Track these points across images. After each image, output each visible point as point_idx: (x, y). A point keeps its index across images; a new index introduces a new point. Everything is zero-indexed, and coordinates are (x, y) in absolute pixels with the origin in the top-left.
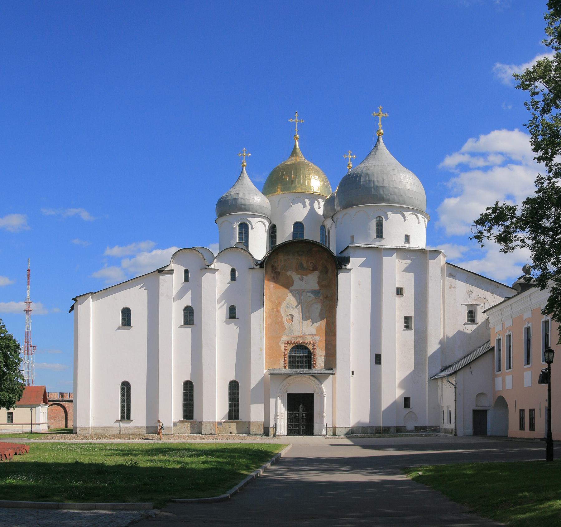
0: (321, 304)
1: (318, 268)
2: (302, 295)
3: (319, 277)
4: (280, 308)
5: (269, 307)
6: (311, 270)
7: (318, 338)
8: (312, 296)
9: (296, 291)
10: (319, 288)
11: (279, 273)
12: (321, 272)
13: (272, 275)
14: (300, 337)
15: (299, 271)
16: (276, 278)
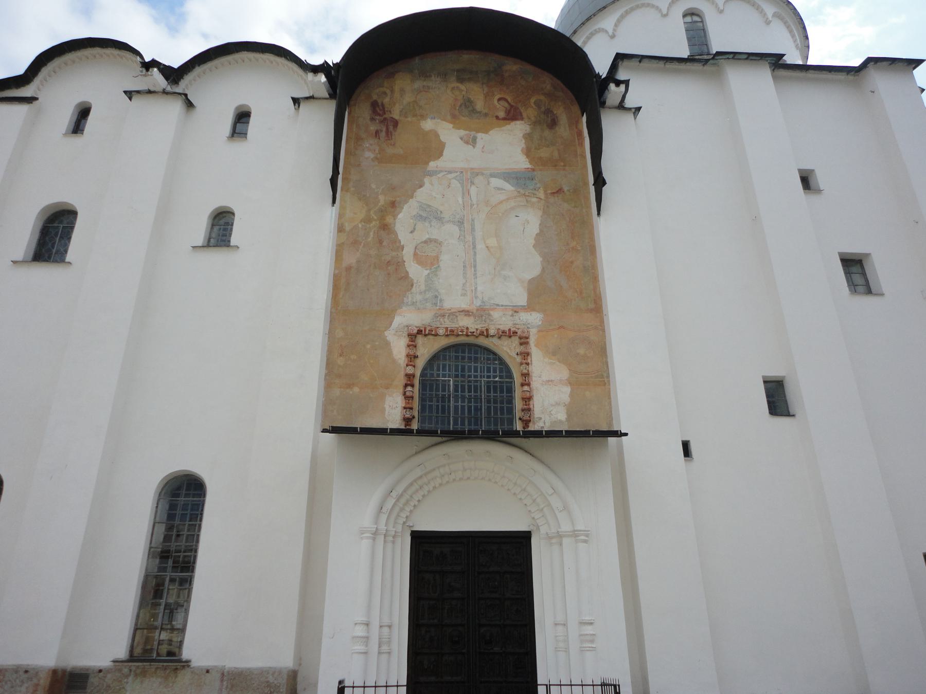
0: (540, 213)
1: (524, 115)
2: (472, 183)
3: (528, 137)
4: (395, 219)
5: (355, 214)
6: (500, 117)
7: (533, 319)
8: (508, 187)
9: (450, 172)
10: (530, 166)
11: (396, 123)
12: (535, 123)
13: (373, 128)
14: (467, 313)
15: (463, 118)
16: (383, 134)
